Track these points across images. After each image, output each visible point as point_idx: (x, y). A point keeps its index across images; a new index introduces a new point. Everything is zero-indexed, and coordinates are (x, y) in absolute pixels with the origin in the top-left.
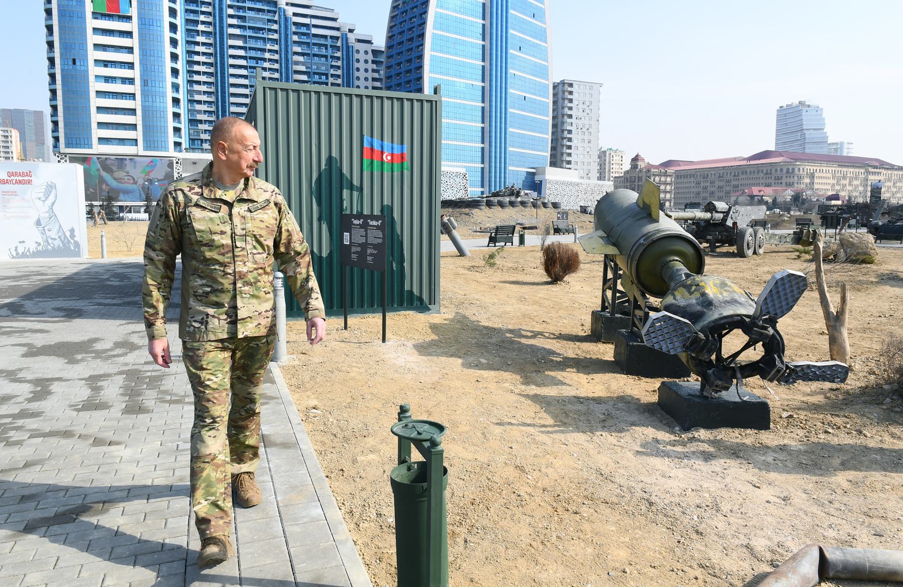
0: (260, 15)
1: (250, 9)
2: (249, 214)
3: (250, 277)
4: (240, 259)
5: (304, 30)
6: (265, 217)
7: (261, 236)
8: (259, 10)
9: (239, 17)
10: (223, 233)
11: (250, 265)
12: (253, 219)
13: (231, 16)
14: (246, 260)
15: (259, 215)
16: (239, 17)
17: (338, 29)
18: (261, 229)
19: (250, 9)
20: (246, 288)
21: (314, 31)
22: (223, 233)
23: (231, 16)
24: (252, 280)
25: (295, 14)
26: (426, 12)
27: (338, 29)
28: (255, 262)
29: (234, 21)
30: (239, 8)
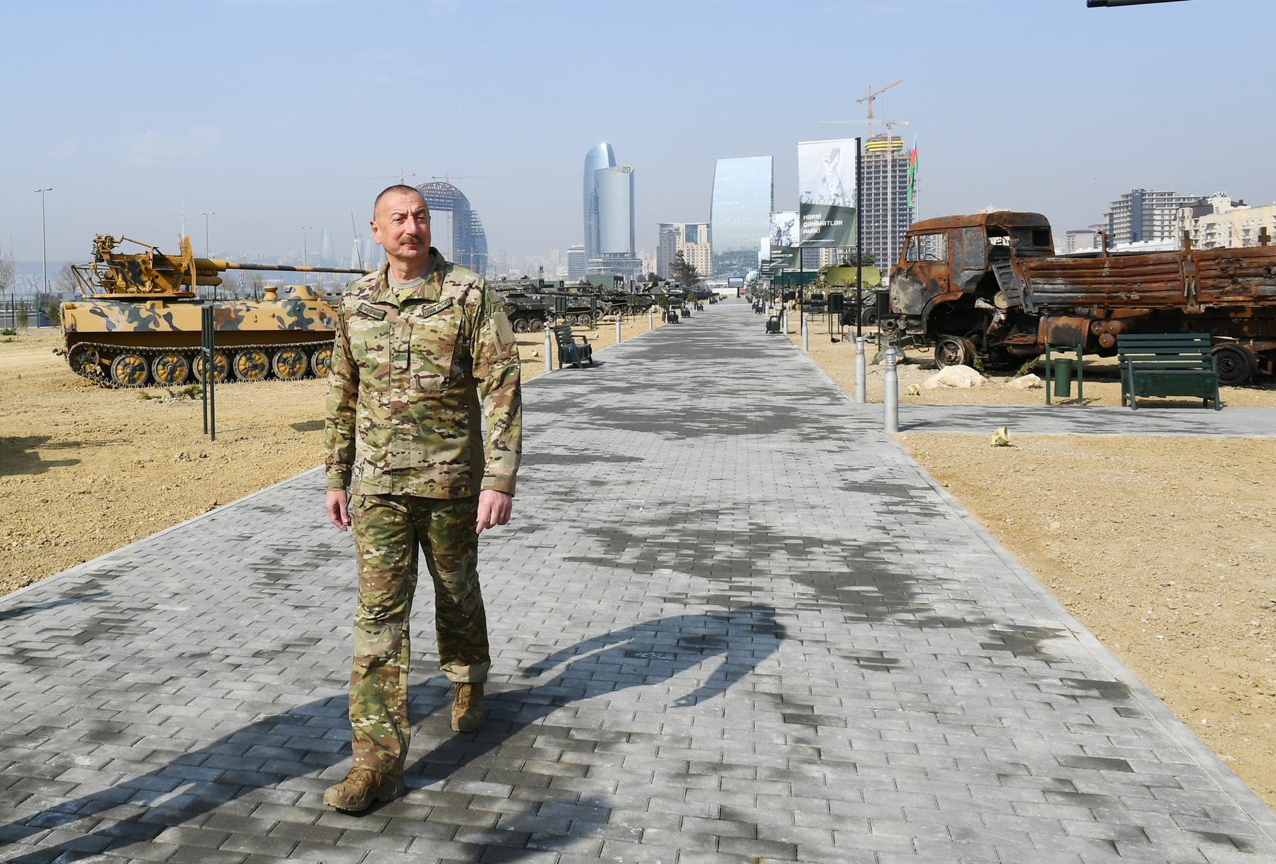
2: (420, 321)
3: (412, 410)
4: (397, 384)
6: (441, 325)
7: (429, 353)
10: (380, 348)
11: (412, 394)
12: (423, 328)
14: (406, 385)
15: (432, 322)
18: (433, 342)
20: (406, 426)
22: (380, 348)
24: (415, 416)
28: (422, 390)
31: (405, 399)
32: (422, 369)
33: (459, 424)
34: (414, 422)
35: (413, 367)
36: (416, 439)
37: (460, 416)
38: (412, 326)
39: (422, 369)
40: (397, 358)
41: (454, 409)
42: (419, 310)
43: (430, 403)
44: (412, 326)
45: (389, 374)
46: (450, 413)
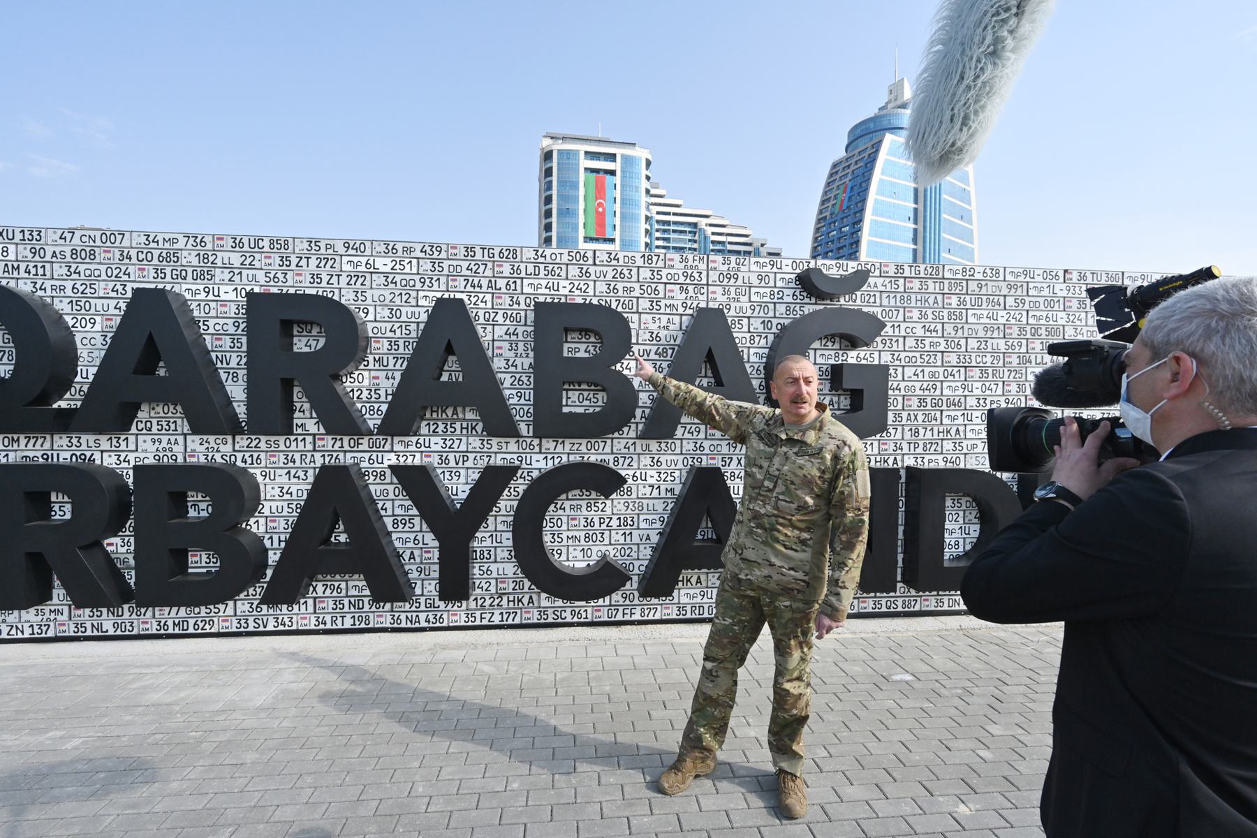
0: (682, 236)
1: (674, 231)
5: (719, 247)
7: (792, 483)
8: (681, 232)
9: (664, 239)
12: (794, 462)
13: (658, 239)
15: (800, 461)
16: (664, 239)
17: (750, 244)
19: (674, 231)
21: (730, 247)
23: (658, 239)
25: (713, 234)
26: (861, 221)
27: (750, 244)
28: (776, 507)
29: (660, 243)
30: (665, 231)
31: (763, 511)
32: (782, 493)
33: (803, 542)
34: (765, 529)
35: (777, 490)
36: (763, 542)
37: (805, 535)
38: (787, 459)
39: (782, 493)
40: (769, 479)
41: (801, 530)
42: (795, 450)
43: (781, 520)
44: (787, 459)
45: (760, 488)
46: (797, 532)
